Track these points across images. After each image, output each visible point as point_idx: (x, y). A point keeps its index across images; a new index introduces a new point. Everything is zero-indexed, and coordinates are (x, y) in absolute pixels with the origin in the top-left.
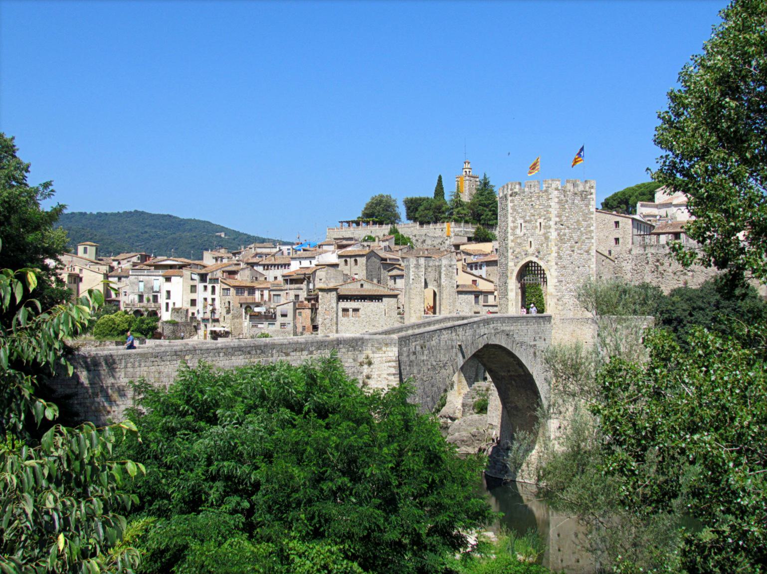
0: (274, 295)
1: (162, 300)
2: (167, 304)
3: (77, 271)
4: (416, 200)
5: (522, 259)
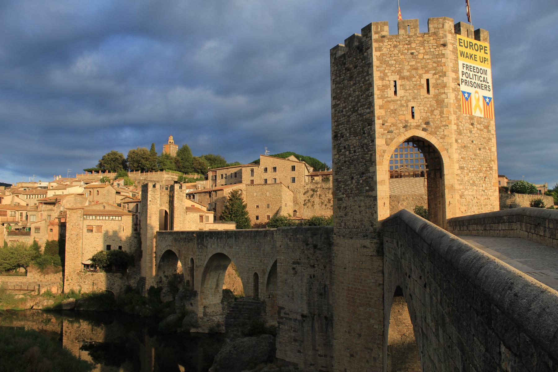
5: (399, 134)
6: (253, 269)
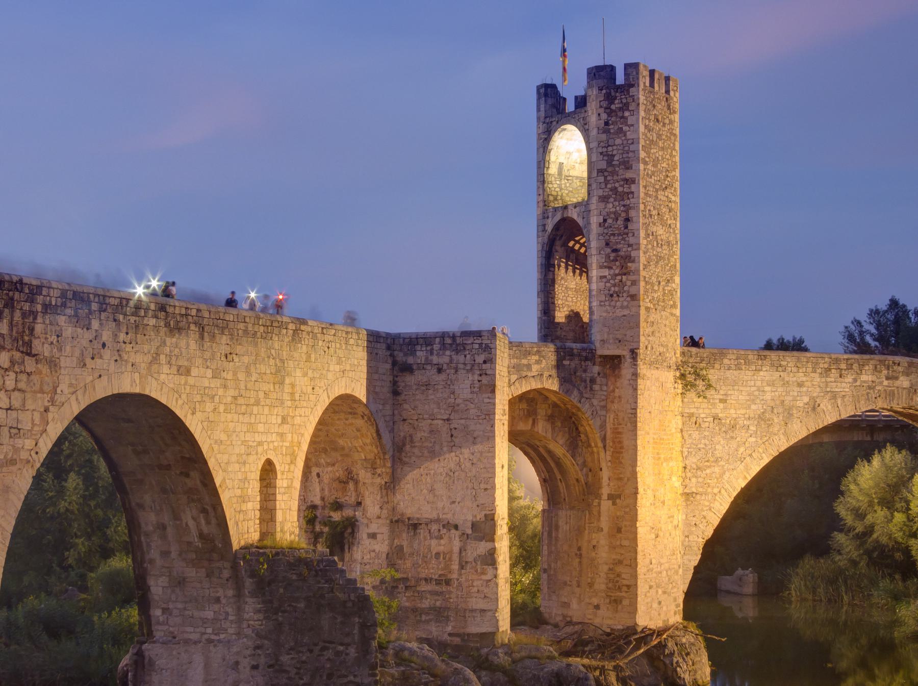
6: (260, 449)
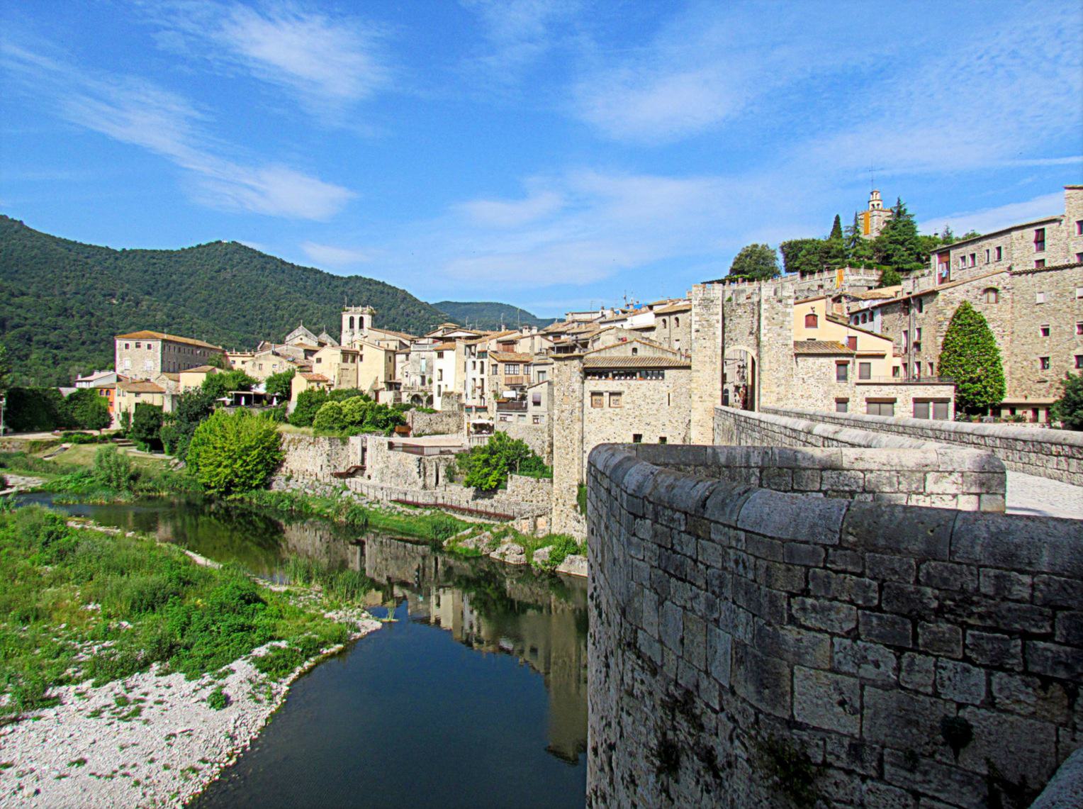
0: (539, 372)
1: (436, 383)
2: (439, 386)
3: (357, 348)
4: (797, 243)
